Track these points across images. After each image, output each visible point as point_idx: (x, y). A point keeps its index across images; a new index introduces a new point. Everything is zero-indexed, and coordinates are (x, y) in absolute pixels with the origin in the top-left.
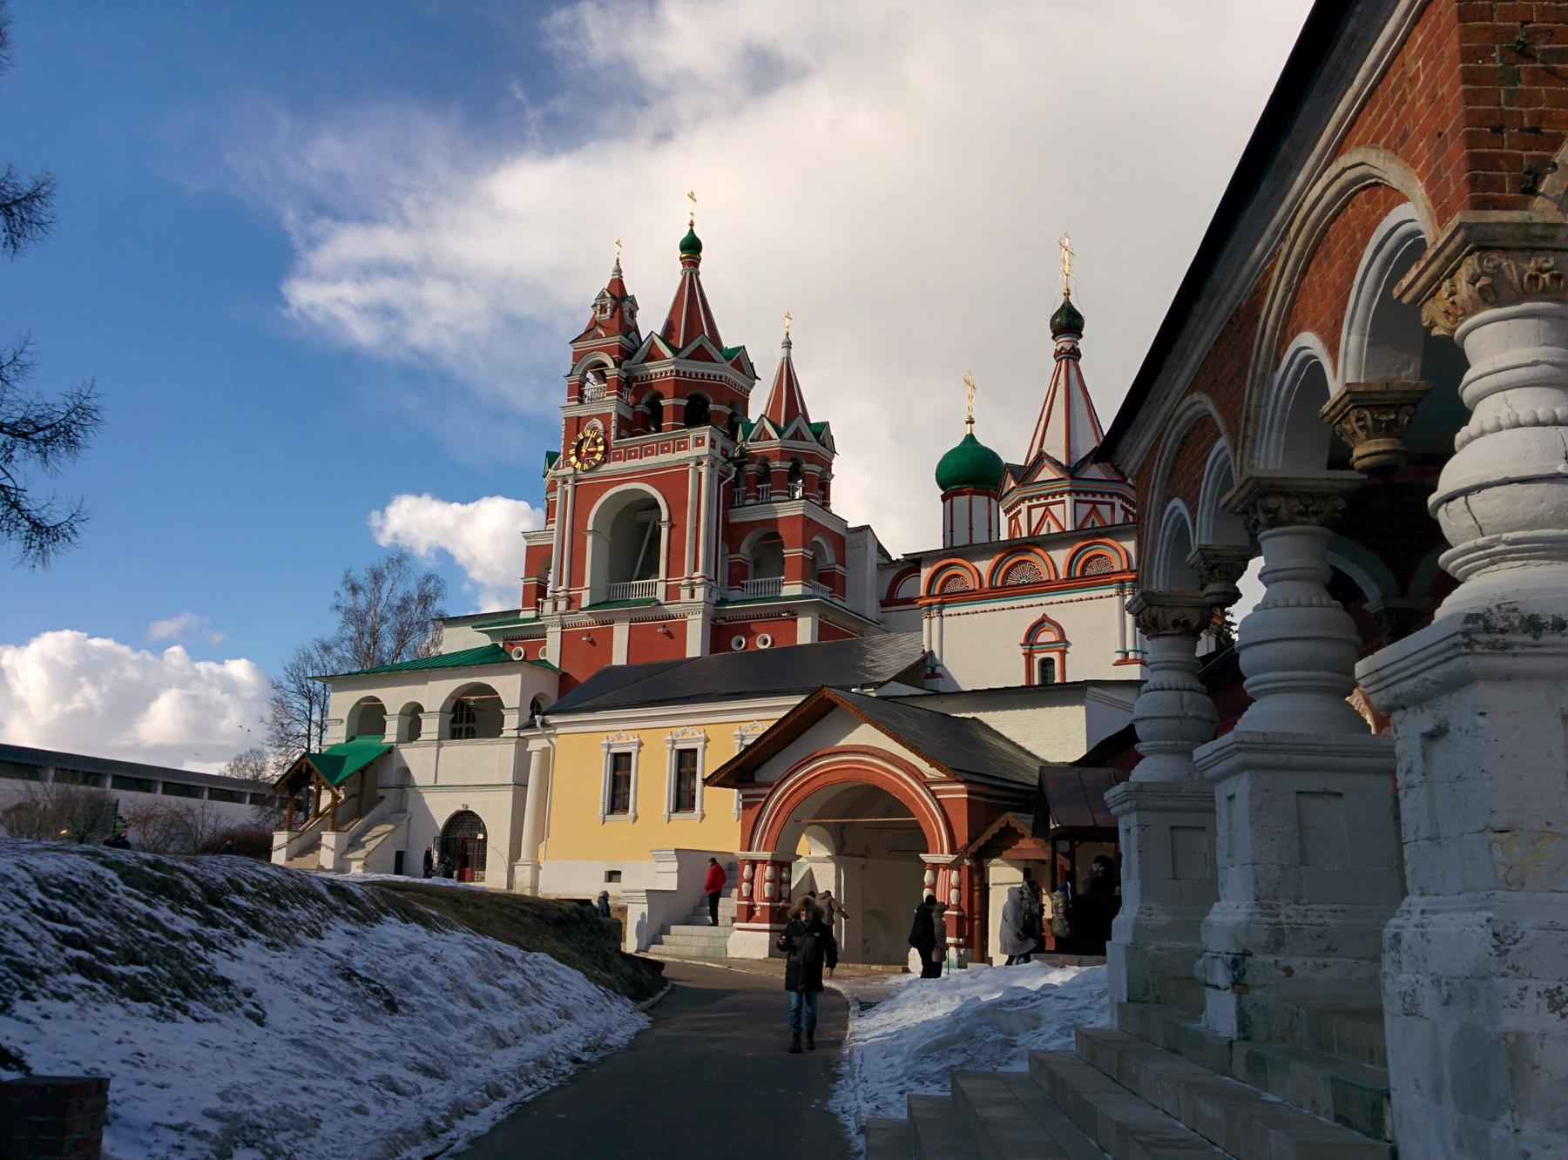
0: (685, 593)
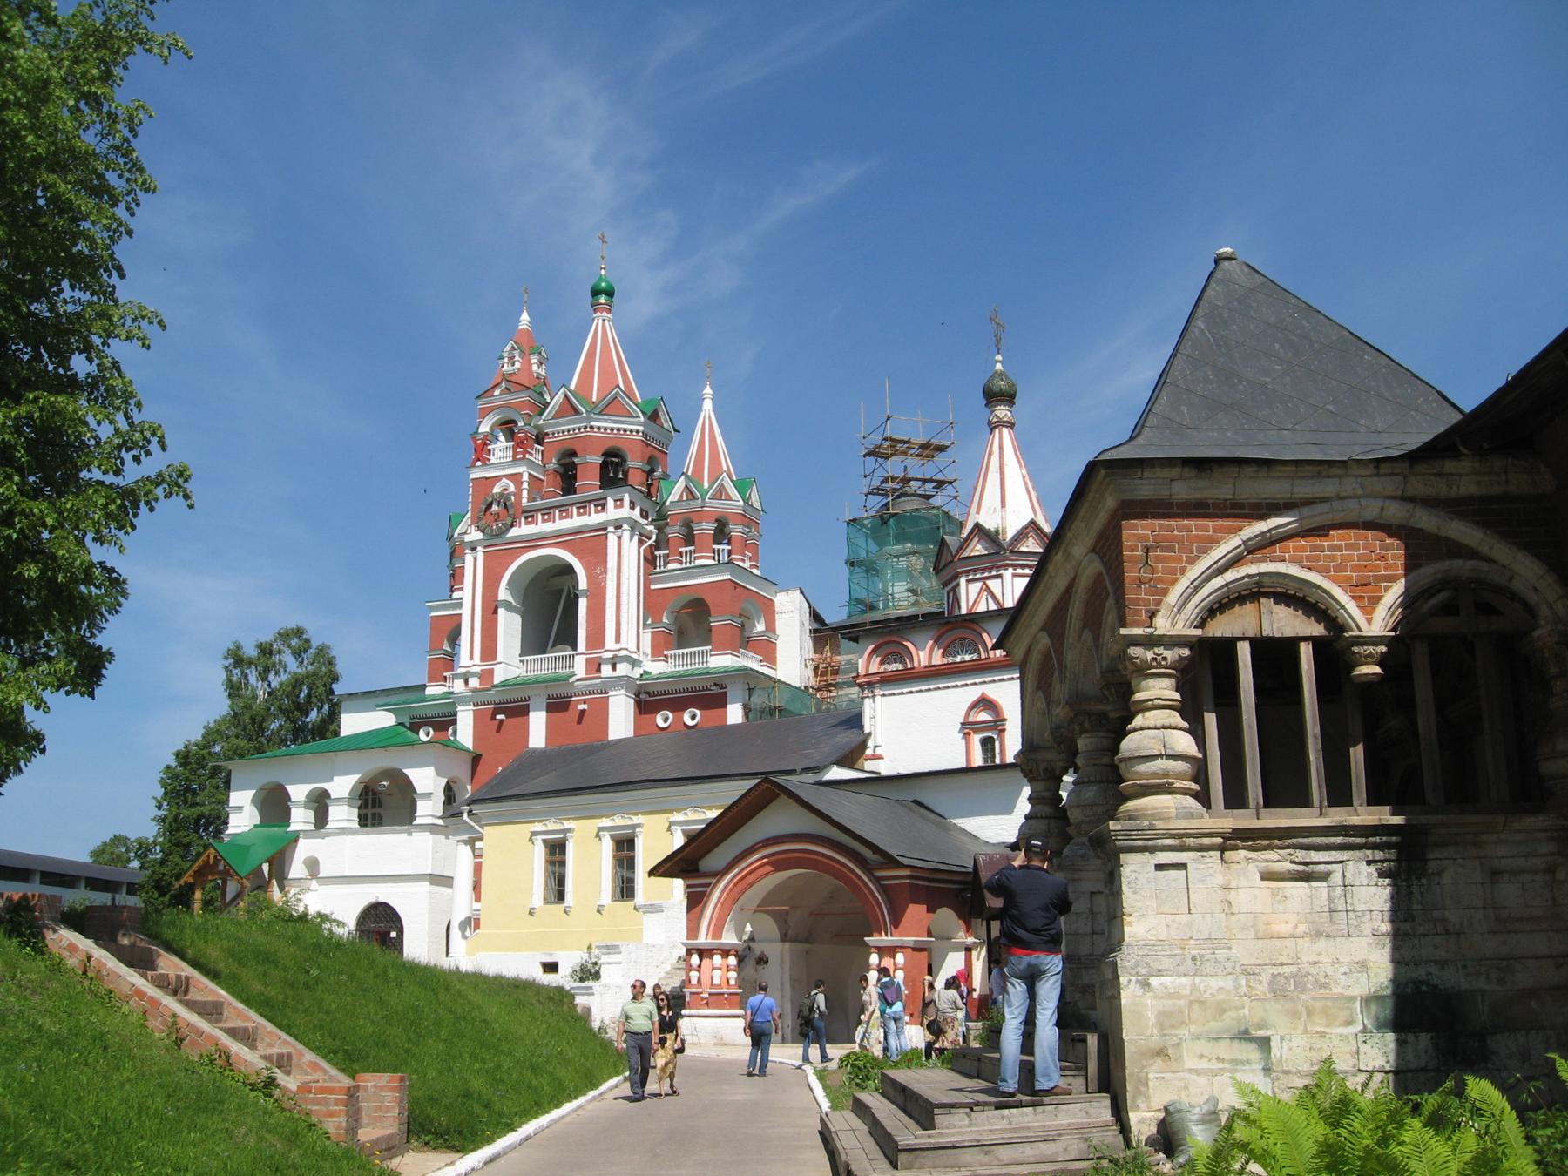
0: (606, 670)
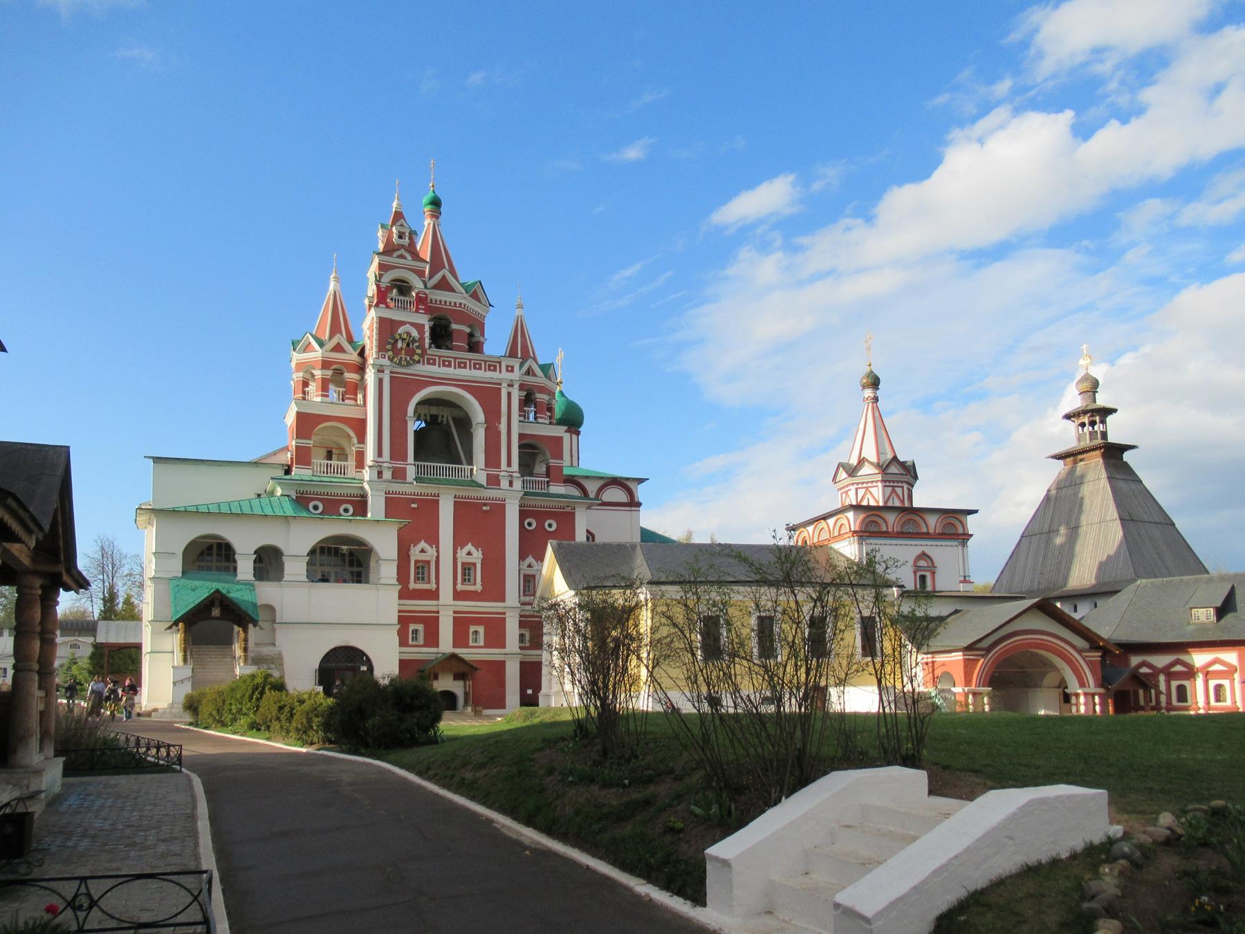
0: (504, 483)
